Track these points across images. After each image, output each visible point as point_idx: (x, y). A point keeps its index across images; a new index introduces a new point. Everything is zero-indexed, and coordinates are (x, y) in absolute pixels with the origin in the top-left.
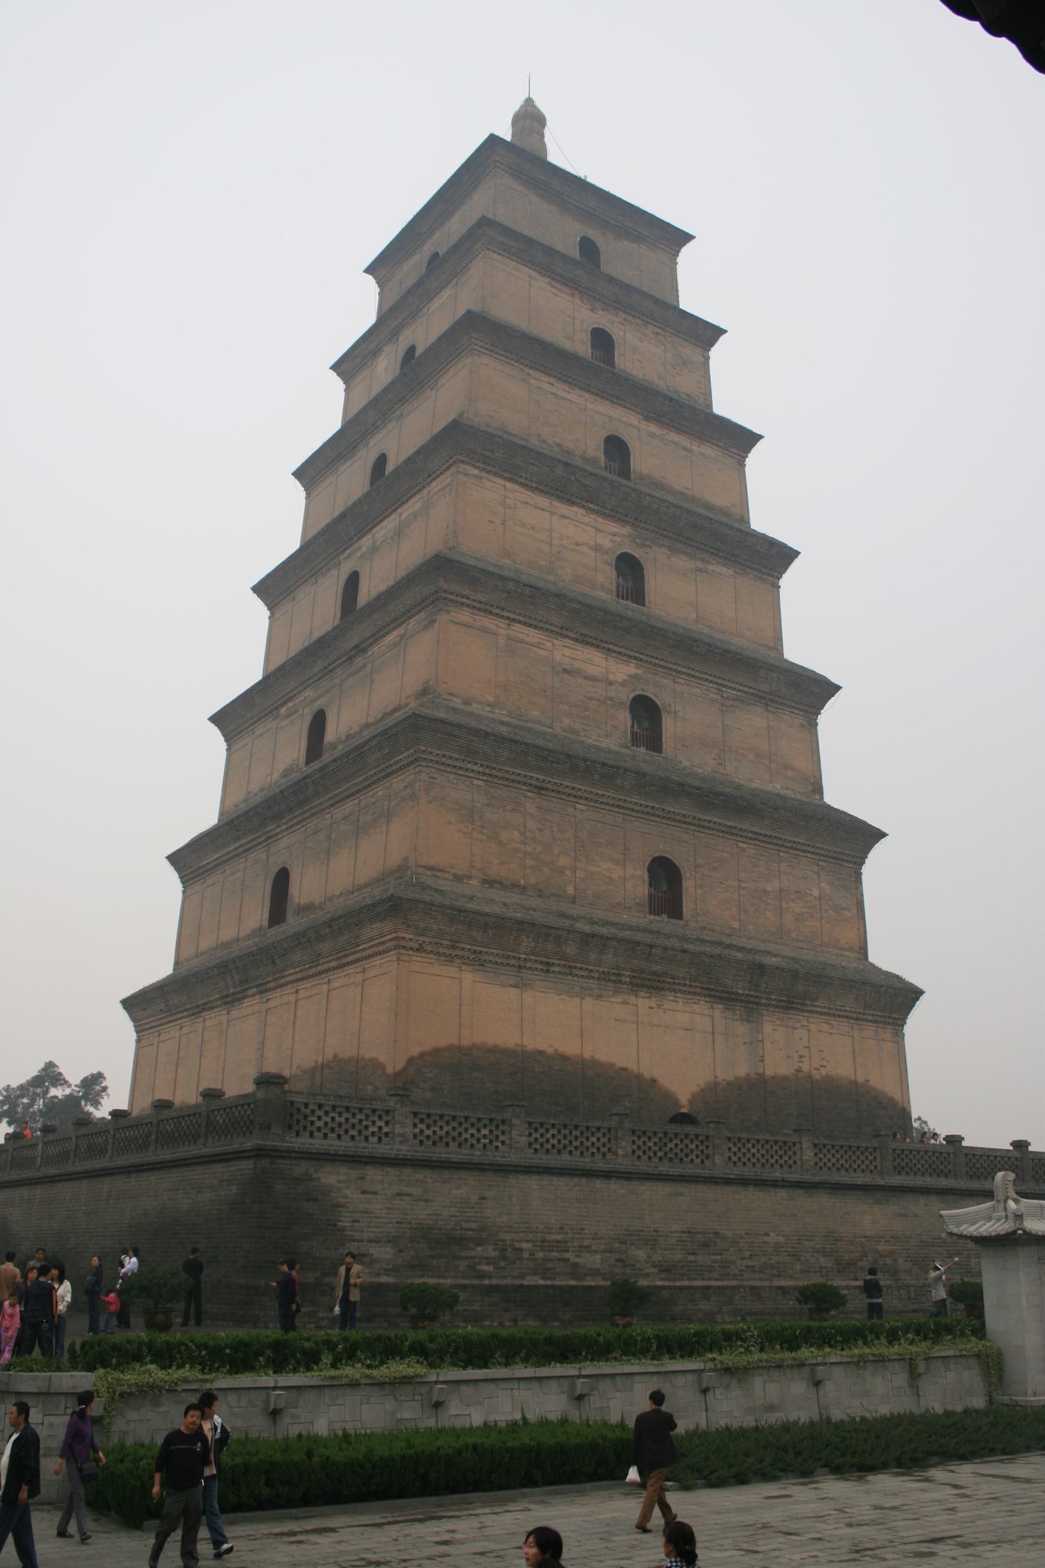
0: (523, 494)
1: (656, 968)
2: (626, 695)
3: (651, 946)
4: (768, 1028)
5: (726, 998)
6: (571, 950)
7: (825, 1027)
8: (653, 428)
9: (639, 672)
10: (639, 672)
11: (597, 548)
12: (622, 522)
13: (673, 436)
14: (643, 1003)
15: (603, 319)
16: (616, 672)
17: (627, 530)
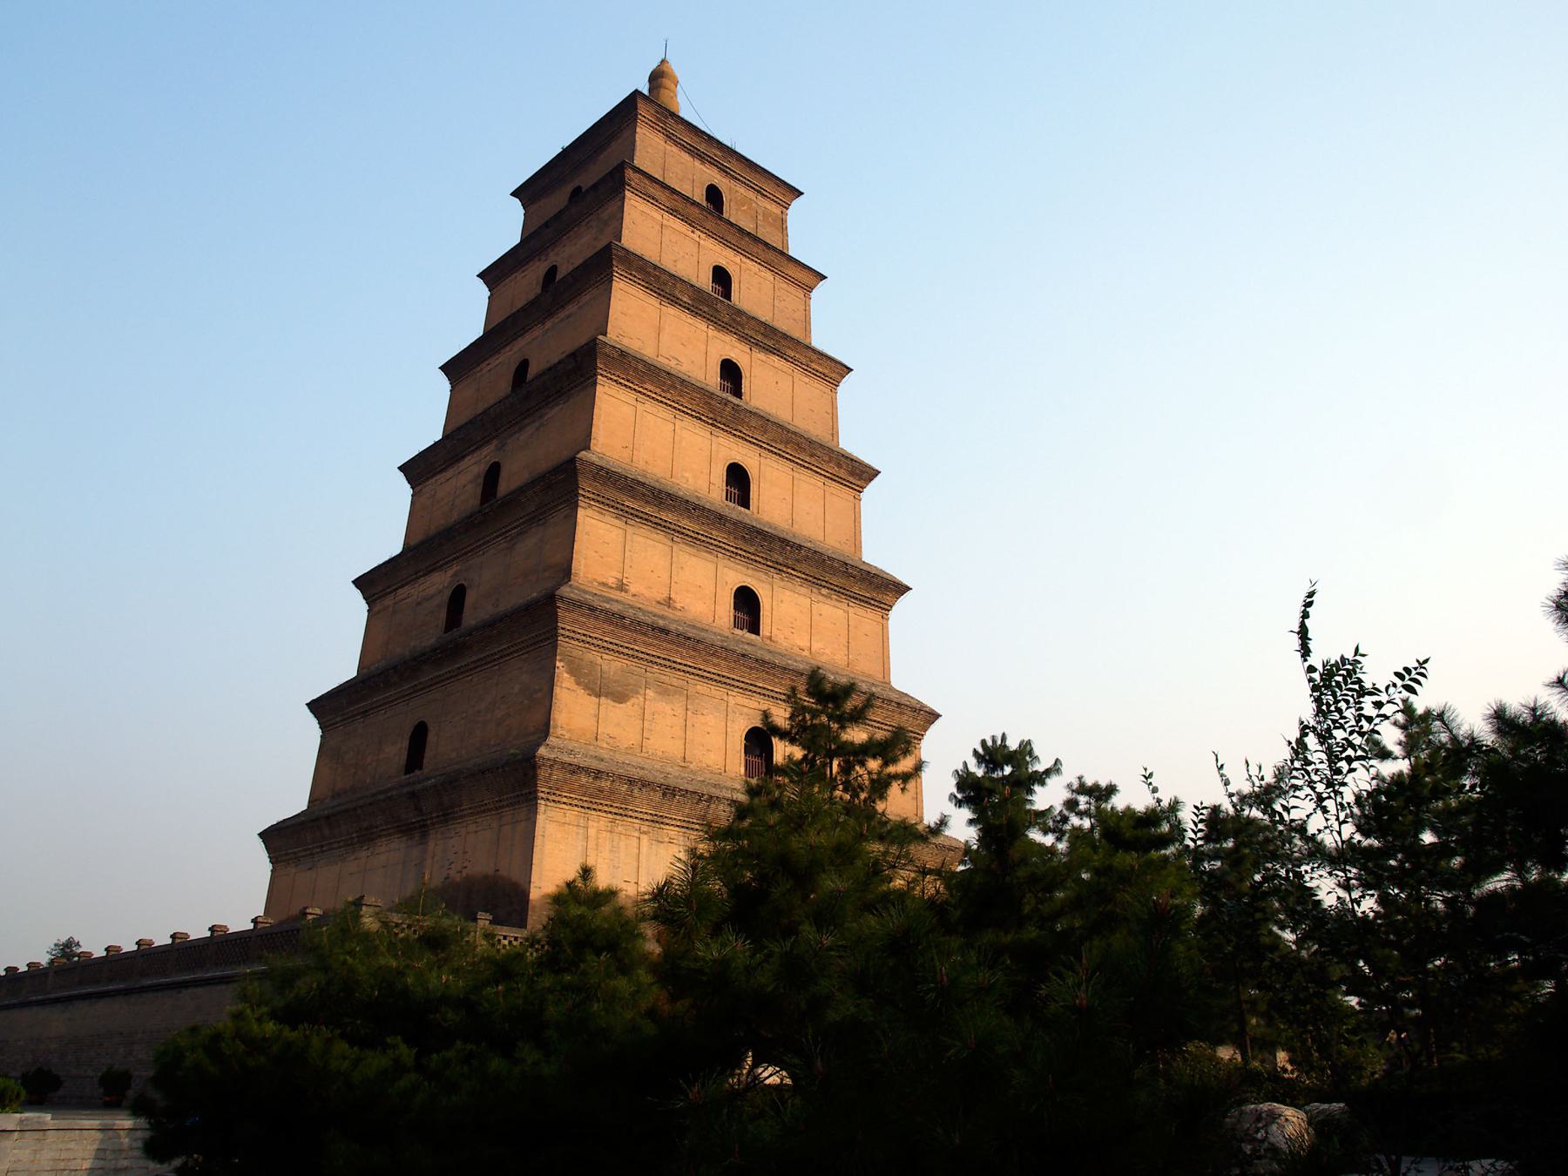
0: (441, 478)
1: (365, 824)
2: (448, 593)
3: (355, 809)
4: (431, 845)
5: (406, 830)
6: (327, 832)
7: (472, 828)
8: (548, 324)
9: (455, 568)
10: (455, 568)
11: (478, 476)
12: (488, 442)
13: (562, 315)
14: (363, 854)
15: (553, 258)
16: (439, 583)
17: (495, 442)
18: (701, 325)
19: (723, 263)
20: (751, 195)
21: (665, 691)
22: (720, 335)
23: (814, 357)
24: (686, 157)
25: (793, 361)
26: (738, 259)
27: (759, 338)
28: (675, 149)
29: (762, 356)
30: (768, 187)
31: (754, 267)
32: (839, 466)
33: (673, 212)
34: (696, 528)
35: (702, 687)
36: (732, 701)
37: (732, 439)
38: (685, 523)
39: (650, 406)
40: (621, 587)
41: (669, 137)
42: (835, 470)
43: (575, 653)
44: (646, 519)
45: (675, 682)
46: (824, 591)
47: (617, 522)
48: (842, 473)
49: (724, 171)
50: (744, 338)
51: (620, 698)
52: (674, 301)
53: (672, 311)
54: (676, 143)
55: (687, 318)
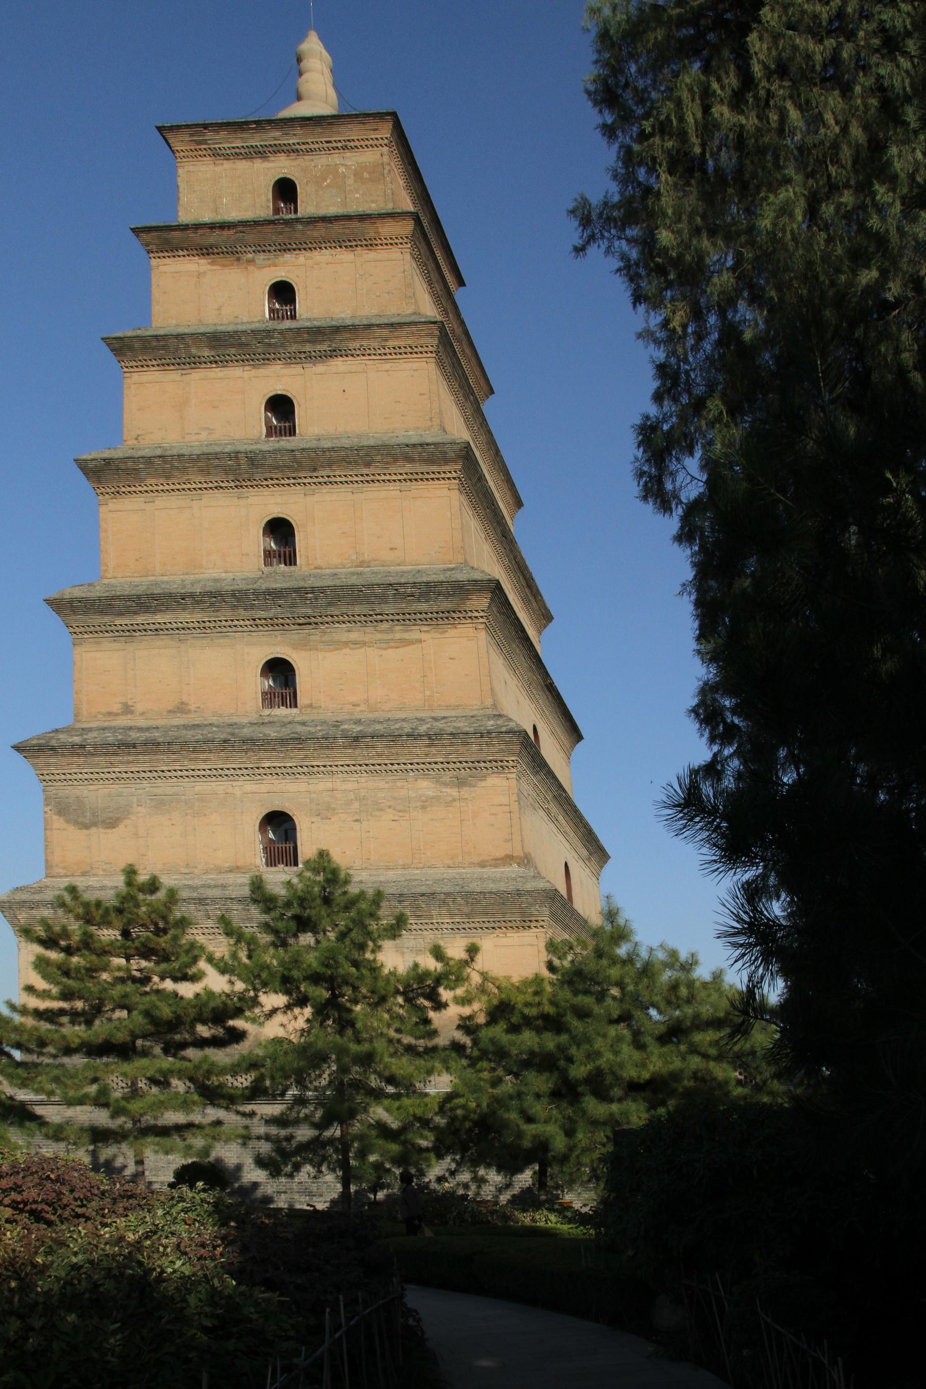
20: (336, 158)
22: (263, 372)
23: (385, 332)
25: (364, 352)
26: (302, 258)
27: (308, 348)
28: (227, 165)
29: (320, 368)
31: (323, 256)
32: (410, 460)
34: (199, 616)
35: (201, 787)
36: (238, 792)
37: (266, 492)
39: (162, 501)
41: (216, 154)
42: (408, 468)
43: (61, 793)
45: (169, 790)
46: (385, 625)
47: (115, 645)
48: (425, 468)
49: (291, 151)
52: (195, 363)
53: (197, 375)
54: (227, 157)
55: (217, 373)
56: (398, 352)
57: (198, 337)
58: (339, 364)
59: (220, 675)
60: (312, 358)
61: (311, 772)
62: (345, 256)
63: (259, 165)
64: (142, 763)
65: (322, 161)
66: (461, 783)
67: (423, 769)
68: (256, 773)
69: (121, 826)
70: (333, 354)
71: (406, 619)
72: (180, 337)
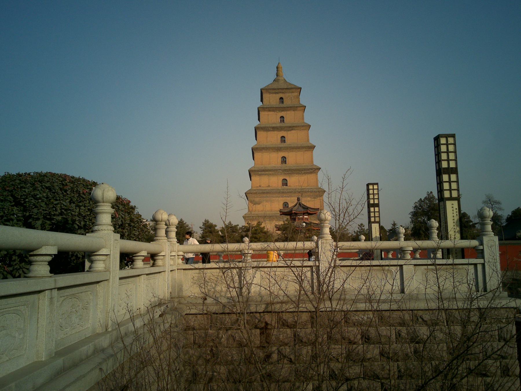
18: (276, 132)
19: (282, 115)
20: (290, 94)
21: (267, 201)
24: (274, 95)
25: (297, 130)
30: (294, 90)
33: (270, 111)
38: (270, 173)
39: (265, 154)
40: (260, 186)
41: (270, 93)
44: (263, 174)
49: (283, 93)
50: (285, 131)
51: (259, 204)
52: (270, 131)
53: (269, 133)
56: (303, 129)
57: (270, 127)
58: (293, 131)
59: (275, 181)
60: (288, 130)
61: (291, 196)
62: (293, 112)
63: (277, 95)
64: (265, 195)
65: (287, 95)
66: (314, 198)
67: (309, 196)
68: (282, 197)
69: (260, 205)
70: (292, 130)
71: (305, 173)
72: (268, 127)
